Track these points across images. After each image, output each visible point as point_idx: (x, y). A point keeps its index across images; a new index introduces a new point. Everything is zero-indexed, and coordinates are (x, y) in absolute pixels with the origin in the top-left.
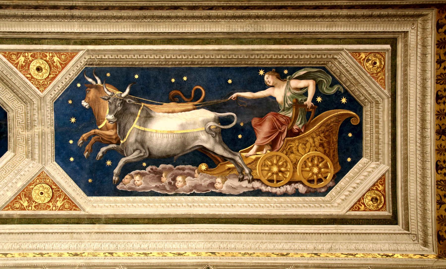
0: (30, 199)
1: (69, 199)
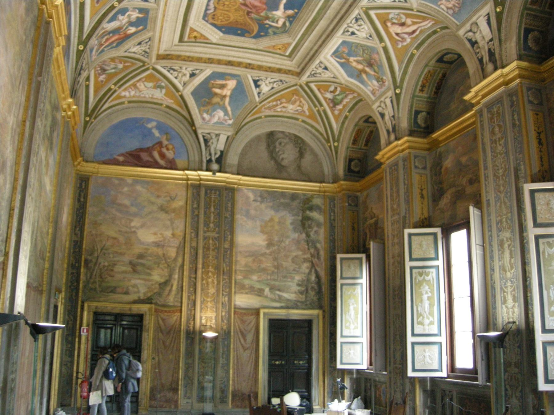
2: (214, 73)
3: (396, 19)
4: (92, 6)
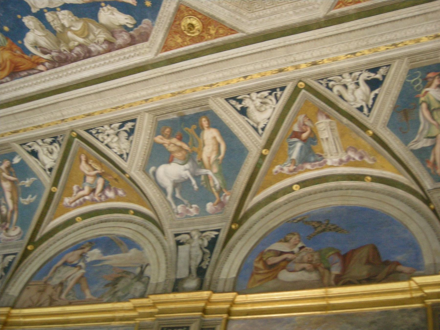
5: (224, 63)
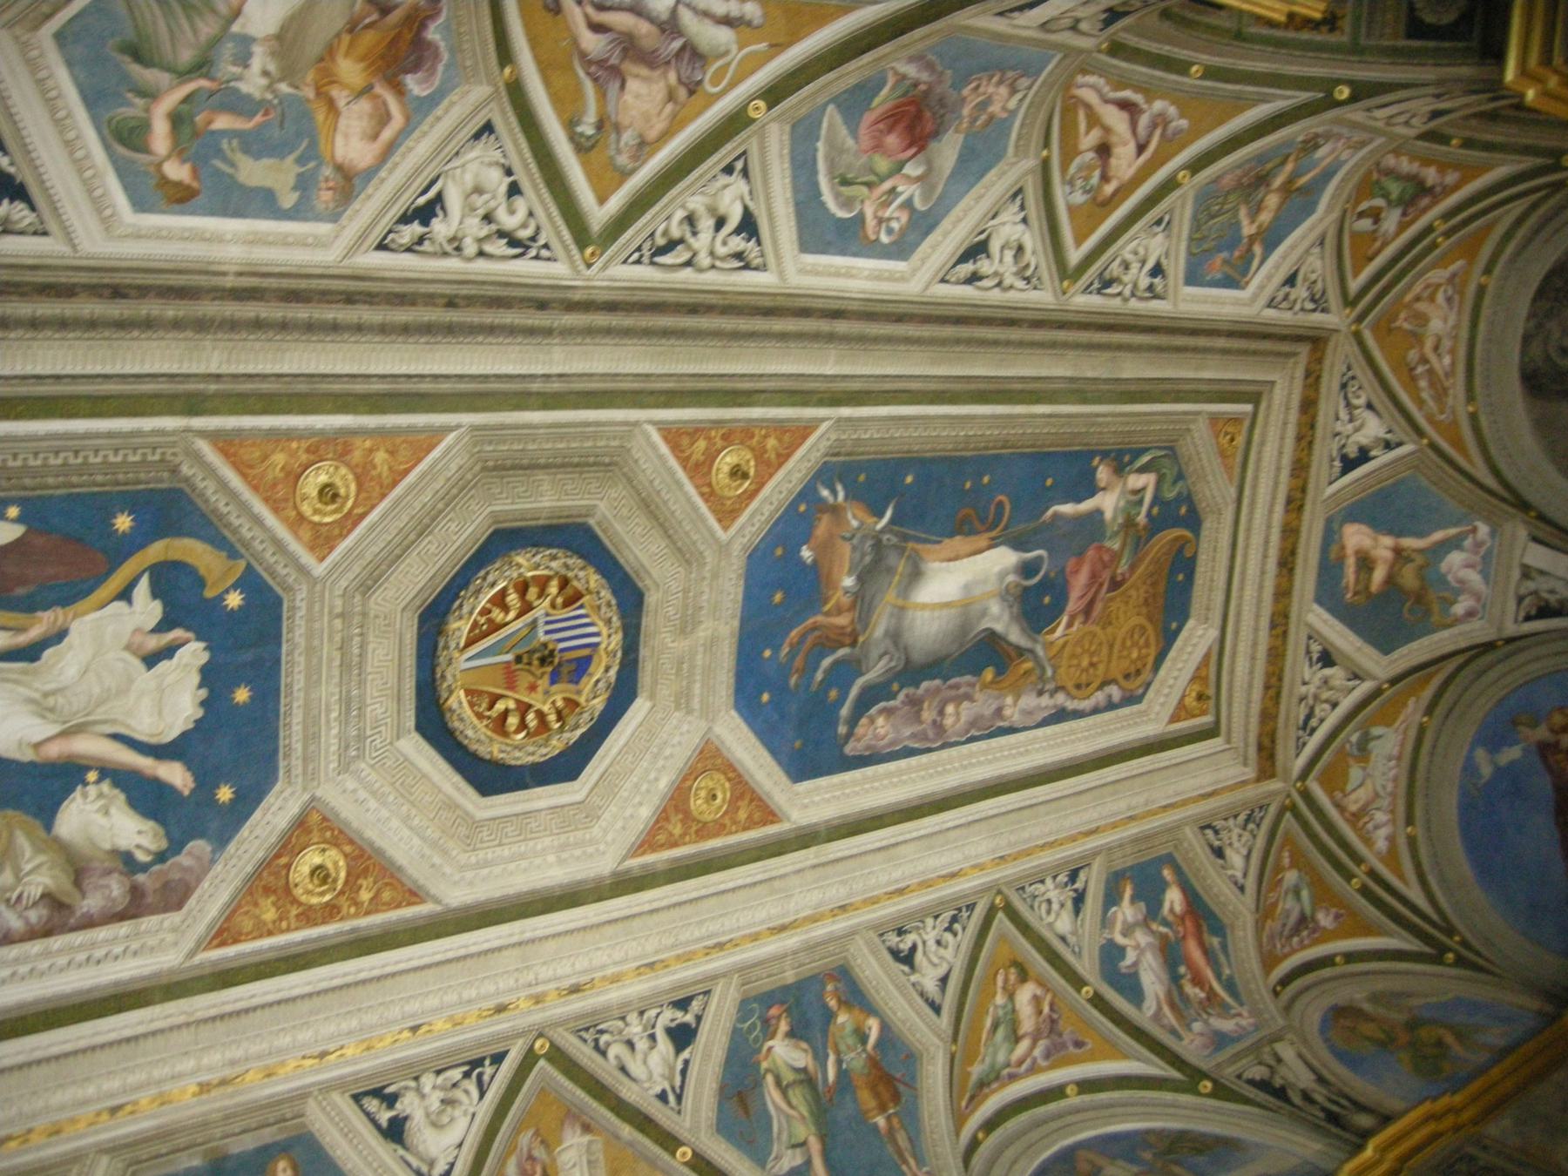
0: (687, 817)
1: (760, 799)
2: (1319, 600)
3: (1087, 179)
4: (1092, 1057)
5: (370, 988)
